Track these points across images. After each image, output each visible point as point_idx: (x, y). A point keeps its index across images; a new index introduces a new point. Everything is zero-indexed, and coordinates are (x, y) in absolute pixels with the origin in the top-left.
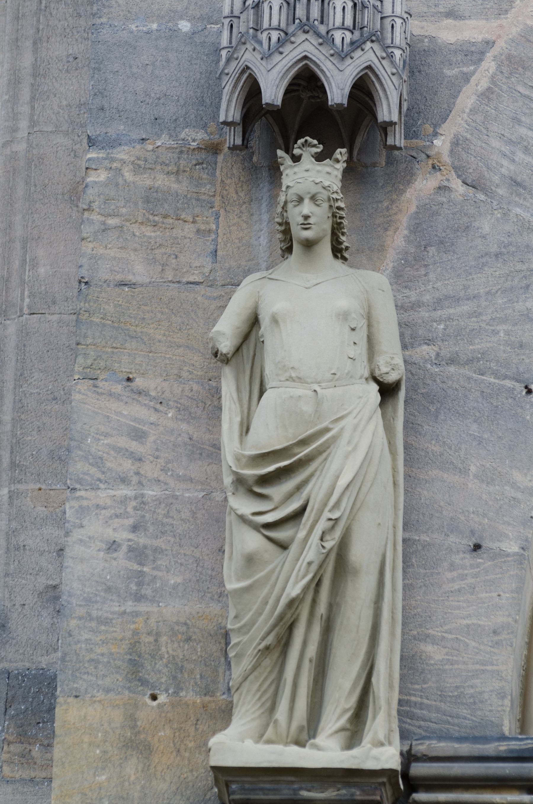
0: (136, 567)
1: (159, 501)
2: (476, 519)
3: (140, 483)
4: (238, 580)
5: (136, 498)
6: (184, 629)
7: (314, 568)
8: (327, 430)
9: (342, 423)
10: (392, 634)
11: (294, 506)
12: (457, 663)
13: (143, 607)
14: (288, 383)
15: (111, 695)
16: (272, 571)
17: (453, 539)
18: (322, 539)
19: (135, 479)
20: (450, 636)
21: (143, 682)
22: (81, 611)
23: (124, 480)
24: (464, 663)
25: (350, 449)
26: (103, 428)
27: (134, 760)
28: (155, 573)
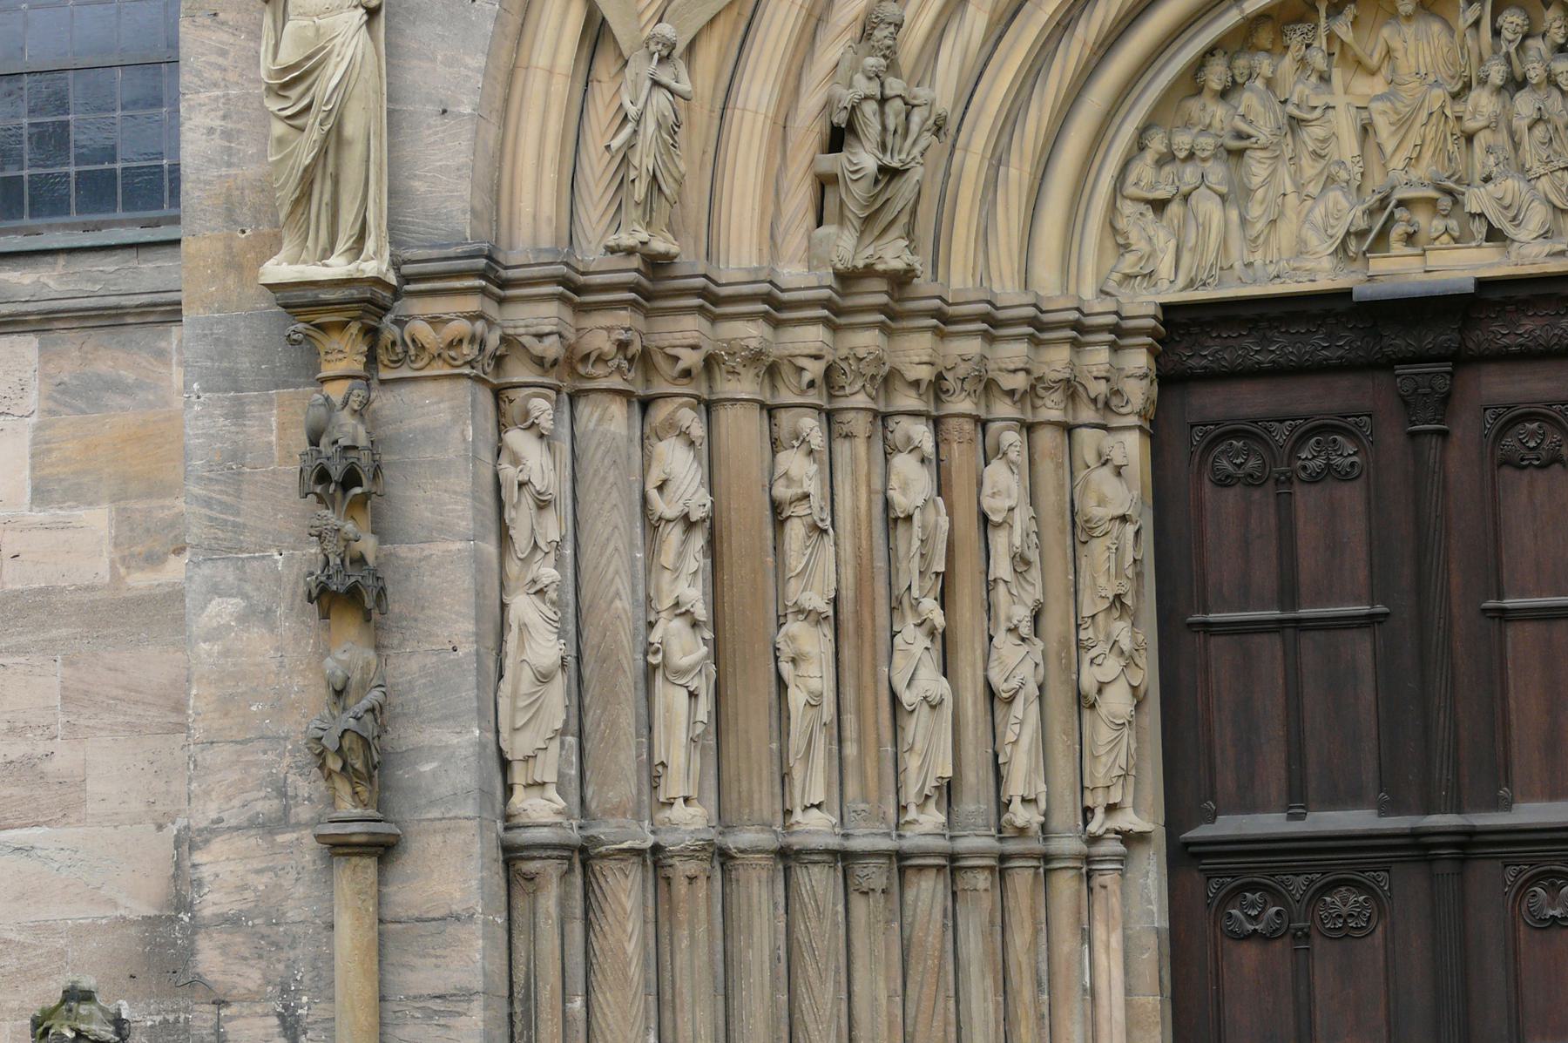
0: (227, 144)
1: (238, 97)
2: (443, 92)
3: (226, 86)
4: (276, 155)
5: (224, 96)
6: (259, 184)
7: (317, 145)
8: (323, 48)
9: (333, 42)
10: (379, 181)
11: (305, 102)
12: (435, 192)
13: (233, 171)
14: (299, 17)
15: (216, 232)
16: (295, 148)
17: (429, 107)
18: (321, 124)
19: (222, 84)
20: (429, 174)
21: (236, 222)
22: (193, 177)
23: (216, 85)
24: (440, 192)
25: (339, 59)
26: (200, 51)
27: (233, 275)
28: (239, 147)
